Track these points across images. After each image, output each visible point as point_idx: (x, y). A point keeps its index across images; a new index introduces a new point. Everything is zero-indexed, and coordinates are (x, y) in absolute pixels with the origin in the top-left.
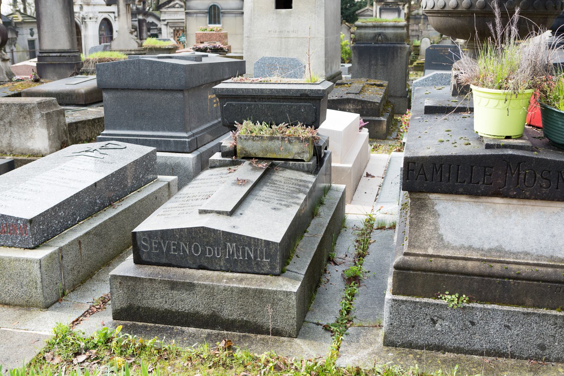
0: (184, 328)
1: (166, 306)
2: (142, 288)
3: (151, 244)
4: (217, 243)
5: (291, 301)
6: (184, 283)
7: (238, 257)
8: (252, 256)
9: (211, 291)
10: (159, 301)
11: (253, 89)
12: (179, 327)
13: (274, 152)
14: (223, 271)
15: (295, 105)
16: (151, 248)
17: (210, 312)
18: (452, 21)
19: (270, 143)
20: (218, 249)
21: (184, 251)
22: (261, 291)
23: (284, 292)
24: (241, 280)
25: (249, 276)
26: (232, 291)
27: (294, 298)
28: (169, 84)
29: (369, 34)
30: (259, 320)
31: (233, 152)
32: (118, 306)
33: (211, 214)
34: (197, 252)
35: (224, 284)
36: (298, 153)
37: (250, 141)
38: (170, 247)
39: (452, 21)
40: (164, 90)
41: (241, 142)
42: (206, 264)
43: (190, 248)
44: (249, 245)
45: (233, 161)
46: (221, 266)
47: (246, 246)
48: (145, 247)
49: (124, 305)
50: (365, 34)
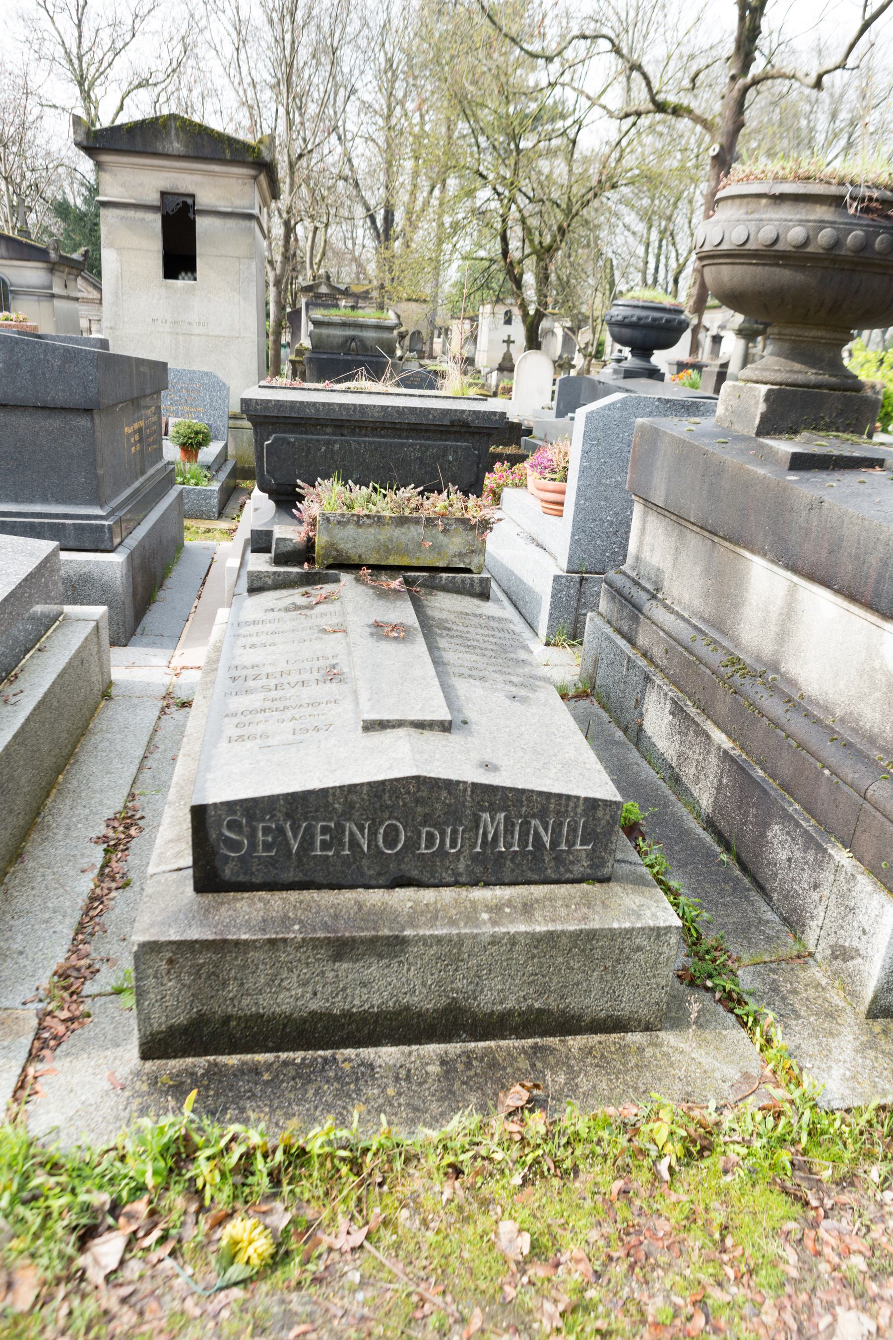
0: (368, 1053)
1: (314, 1005)
2: (244, 967)
3: (252, 836)
4: (453, 815)
5: (665, 949)
6: (373, 941)
7: (508, 845)
8: (547, 839)
9: (452, 951)
10: (293, 994)
11: (341, 405)
12: (350, 1052)
13: (406, 552)
14: (463, 885)
15: (435, 445)
16: (253, 845)
17: (444, 1002)
18: (784, 276)
19: (397, 532)
20: (454, 832)
21: (354, 844)
22: (592, 935)
23: (652, 929)
24: (527, 909)
25: (539, 891)
26: (514, 944)
27: (673, 941)
28: (58, 395)
29: (334, 336)
30: (574, 1003)
31: (305, 553)
32: (159, 1022)
33: (401, 732)
34: (391, 841)
35: (488, 930)
36: (461, 555)
37: (351, 528)
38: (313, 837)
39: (784, 276)
40: (43, 408)
41: (328, 530)
42: (415, 873)
43: (373, 834)
44: (543, 815)
45: (307, 574)
46: (457, 875)
47: (534, 816)
48: (234, 845)
49: (181, 1018)
50: (328, 336)
